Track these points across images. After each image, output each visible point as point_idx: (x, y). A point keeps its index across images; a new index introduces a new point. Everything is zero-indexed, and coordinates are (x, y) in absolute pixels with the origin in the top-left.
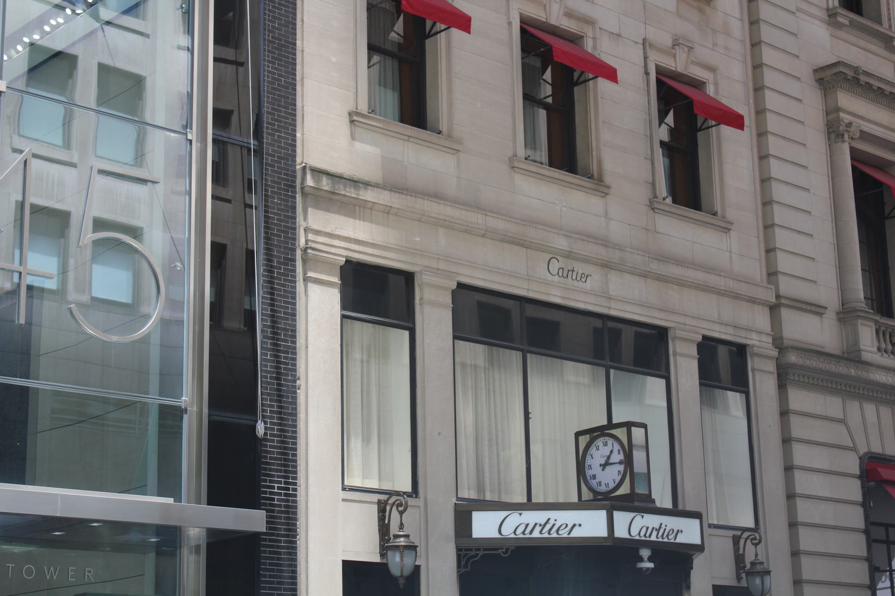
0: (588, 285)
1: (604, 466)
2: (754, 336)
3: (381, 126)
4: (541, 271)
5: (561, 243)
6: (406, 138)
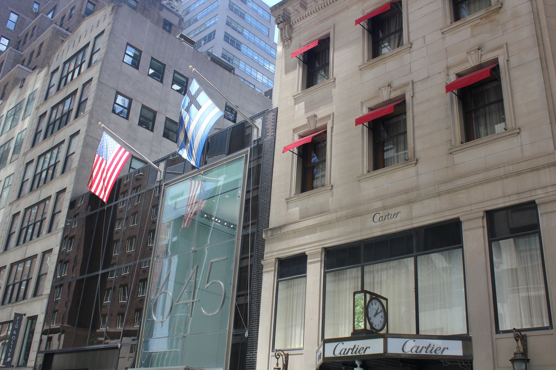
1: (375, 315)
2: (539, 192)
4: (370, 223)
5: (379, 204)
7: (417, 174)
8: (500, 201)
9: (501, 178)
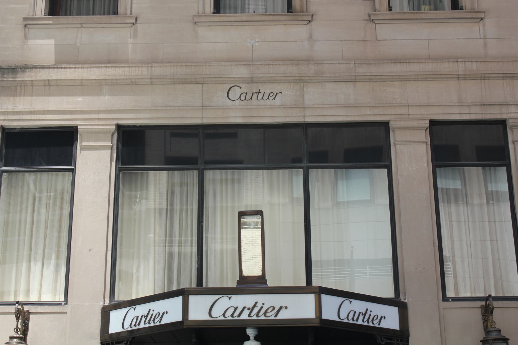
0: (278, 101)
3: (51, 22)
5: (242, 72)
6: (79, 26)
7: (310, 38)
8: (456, 110)
9: (458, 78)
